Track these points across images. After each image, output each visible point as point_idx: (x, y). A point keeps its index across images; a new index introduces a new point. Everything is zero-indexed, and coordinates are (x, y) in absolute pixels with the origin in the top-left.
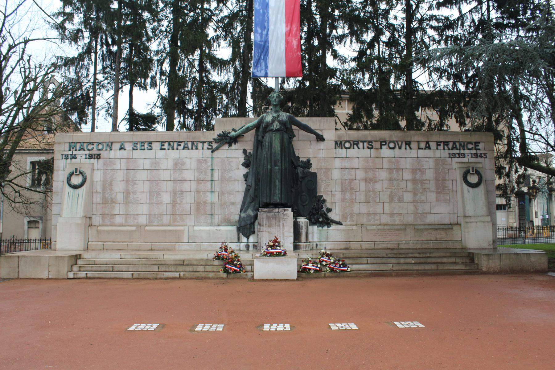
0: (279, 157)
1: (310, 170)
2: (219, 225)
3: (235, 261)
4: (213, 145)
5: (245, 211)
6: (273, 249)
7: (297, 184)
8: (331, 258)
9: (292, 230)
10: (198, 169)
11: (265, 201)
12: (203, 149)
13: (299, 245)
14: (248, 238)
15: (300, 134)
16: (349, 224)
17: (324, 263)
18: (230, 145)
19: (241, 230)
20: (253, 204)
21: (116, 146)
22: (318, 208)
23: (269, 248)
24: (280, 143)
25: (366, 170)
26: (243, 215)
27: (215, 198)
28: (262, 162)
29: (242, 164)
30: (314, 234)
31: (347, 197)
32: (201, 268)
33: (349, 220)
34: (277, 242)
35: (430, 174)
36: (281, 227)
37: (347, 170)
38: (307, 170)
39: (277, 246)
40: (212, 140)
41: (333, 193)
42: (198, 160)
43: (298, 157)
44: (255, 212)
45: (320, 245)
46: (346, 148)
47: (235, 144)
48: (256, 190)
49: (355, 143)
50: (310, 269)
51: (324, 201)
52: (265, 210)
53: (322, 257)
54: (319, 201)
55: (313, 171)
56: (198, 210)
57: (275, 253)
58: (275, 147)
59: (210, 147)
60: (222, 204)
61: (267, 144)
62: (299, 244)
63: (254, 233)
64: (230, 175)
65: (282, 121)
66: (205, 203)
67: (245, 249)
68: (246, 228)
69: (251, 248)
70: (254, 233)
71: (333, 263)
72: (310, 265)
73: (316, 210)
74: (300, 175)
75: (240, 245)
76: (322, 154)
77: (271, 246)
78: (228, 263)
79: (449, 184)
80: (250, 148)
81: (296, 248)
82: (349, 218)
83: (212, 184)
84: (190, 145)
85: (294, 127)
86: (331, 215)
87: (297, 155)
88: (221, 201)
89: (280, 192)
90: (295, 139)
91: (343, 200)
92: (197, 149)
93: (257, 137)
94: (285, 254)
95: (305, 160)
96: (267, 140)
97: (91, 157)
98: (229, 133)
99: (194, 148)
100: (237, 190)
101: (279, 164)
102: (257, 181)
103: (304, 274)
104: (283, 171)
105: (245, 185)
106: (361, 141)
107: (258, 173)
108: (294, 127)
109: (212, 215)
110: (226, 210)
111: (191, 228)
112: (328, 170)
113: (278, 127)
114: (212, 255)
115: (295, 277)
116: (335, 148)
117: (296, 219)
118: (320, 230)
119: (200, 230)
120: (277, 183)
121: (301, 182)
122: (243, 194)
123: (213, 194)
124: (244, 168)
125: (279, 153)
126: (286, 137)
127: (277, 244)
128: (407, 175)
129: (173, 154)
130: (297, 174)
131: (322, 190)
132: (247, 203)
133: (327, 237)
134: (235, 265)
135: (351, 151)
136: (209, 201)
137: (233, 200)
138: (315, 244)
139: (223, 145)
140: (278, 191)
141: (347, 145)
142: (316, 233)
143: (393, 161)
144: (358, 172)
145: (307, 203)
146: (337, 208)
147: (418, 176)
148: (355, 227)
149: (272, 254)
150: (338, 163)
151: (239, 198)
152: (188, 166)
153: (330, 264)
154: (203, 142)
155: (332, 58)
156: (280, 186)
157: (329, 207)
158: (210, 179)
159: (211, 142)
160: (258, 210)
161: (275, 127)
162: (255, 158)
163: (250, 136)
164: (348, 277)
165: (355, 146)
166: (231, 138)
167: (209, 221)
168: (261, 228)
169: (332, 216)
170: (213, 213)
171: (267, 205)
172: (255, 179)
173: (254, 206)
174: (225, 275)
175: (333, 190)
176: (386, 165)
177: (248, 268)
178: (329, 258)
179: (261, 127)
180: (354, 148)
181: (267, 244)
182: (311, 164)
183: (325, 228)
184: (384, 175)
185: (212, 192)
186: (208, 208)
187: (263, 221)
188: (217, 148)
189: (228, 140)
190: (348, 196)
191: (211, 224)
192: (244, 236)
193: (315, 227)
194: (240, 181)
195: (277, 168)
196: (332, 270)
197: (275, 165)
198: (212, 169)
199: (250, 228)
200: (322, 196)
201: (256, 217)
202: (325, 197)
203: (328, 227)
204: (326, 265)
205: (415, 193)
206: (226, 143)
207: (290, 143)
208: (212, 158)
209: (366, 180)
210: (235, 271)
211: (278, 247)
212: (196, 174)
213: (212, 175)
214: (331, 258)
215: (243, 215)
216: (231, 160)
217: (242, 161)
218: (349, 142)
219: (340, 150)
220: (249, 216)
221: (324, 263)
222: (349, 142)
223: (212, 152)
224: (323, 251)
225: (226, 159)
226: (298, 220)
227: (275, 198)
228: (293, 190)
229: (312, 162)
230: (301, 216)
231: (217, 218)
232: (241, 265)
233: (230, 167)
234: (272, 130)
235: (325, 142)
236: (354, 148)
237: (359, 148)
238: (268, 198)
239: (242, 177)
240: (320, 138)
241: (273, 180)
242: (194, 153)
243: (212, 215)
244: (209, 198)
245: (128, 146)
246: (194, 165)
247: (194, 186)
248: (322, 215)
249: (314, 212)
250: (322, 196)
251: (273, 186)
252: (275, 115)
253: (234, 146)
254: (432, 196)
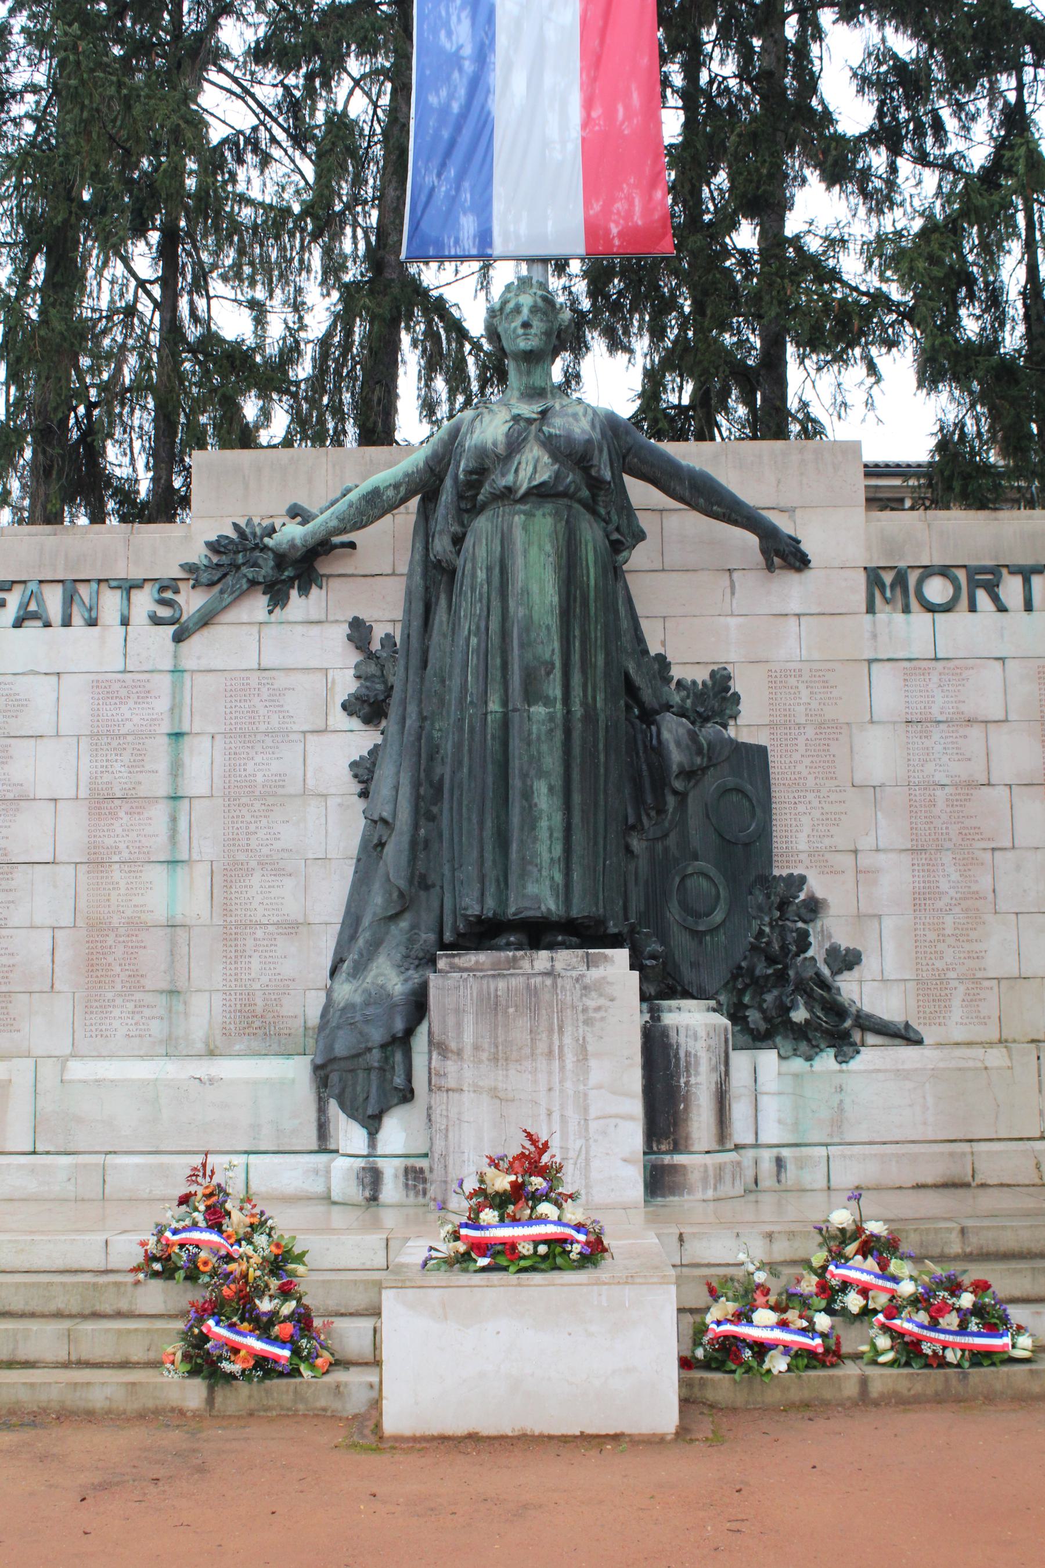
0: (550, 648)
1: (731, 732)
2: (211, 1053)
3: (261, 1292)
4: (180, 599)
5: (359, 969)
6: (515, 1221)
7: (661, 811)
8: (895, 1266)
9: (634, 1079)
10: (102, 737)
11: (475, 910)
12: (125, 622)
13: (674, 1169)
14: (372, 1123)
16: (958, 1035)
17: (854, 1302)
18: (278, 597)
19: (334, 1078)
20: (404, 924)
22: (784, 948)
23: (489, 1216)
24: (558, 568)
26: (345, 991)
27: (191, 898)
28: (455, 683)
29: (344, 707)
30: (764, 1101)
31: (944, 886)
32: (43, 1339)
33: (957, 1012)
34: (542, 1171)
36: (570, 1058)
37: (936, 733)
38: (710, 730)
39: (537, 1198)
40: (180, 574)
41: (864, 861)
42: (96, 685)
43: (662, 661)
44: (415, 977)
45: (801, 1163)
46: (931, 608)
47: (304, 591)
48: (417, 846)
50: (761, 1349)
51: (814, 907)
52: (471, 958)
53: (838, 1257)
54: (783, 905)
55: (746, 737)
56: (94, 968)
57: (525, 1249)
58: (526, 592)
59: (164, 612)
60: (233, 933)
61: (481, 575)
62: (679, 1159)
63: (407, 1095)
64: (275, 767)
65: (569, 439)
66: (137, 926)
67: (356, 1193)
68: (366, 1069)
69: (391, 1190)
70: (407, 1095)
71: (916, 1302)
72: (764, 1316)
73: (771, 960)
74: (676, 757)
75: (328, 1172)
76: (793, 645)
77: (501, 1201)
78: (215, 1309)
80: (387, 611)
82: (956, 1003)
83: (174, 819)
84: (53, 600)
85: (640, 493)
86: (855, 990)
87: (654, 648)
88: (227, 911)
89: (558, 850)
90: (639, 557)
91: (922, 899)
92: (92, 623)
93: (427, 549)
94: (595, 1251)
95: (700, 675)
96: (481, 552)
98: (271, 531)
99: (77, 619)
101: (555, 690)
102: (429, 795)
103: (720, 1385)
104: (578, 726)
105: (363, 822)
106: (1014, 570)
107: (433, 753)
108: (640, 493)
109: (173, 992)
110: (255, 964)
111: (48, 1071)
113: (543, 476)
114: (128, 1249)
115: (664, 1415)
116: (871, 609)
117: (655, 1014)
118: (796, 1076)
119: (98, 1082)
120: (545, 800)
121: (682, 797)
122: (349, 871)
123: (181, 871)
124: (355, 723)
125: (553, 621)
126: (591, 535)
127: (538, 1182)
130: (658, 751)
131: (802, 846)
132: (366, 922)
133: (838, 1119)
134: (263, 1326)
135: (959, 620)
136: (160, 915)
137: (292, 909)
138: (767, 1157)
139: (242, 595)
140: (547, 848)
141: (937, 590)
142: (772, 1087)
144: (1000, 738)
145: (718, 916)
146: (889, 946)
148: (996, 1057)
149: (504, 1257)
150: (887, 691)
151: (326, 898)
152: (40, 720)
153: (892, 1311)
154: (129, 587)
155: (823, 186)
156: (558, 818)
157: (844, 941)
158: (163, 789)
159: (168, 586)
160: (432, 961)
161: (525, 474)
162: (415, 661)
163: (389, 544)
164: (1023, 1399)
165: (982, 597)
166: (281, 559)
167: (156, 1028)
168: (451, 1066)
170: (182, 984)
171: (484, 933)
172: (416, 785)
173: (411, 941)
174: (193, 1393)
175: (866, 843)
177: (352, 1336)
178: (883, 1266)
179: (448, 482)
180: (973, 608)
181: (471, 1184)
182: (736, 698)
183: (826, 1061)
185: (173, 863)
186: (153, 954)
187: (459, 1025)
188: (206, 619)
189: (267, 568)
190: (949, 877)
191: (171, 1047)
192: (352, 1113)
193: (768, 1058)
194: (332, 802)
195: (539, 710)
196: (910, 1350)
197: (532, 694)
198: (177, 736)
199: (385, 1069)
200: (803, 879)
201: (418, 1006)
202: (817, 885)
203: (842, 1058)
204: (867, 1312)
206: (253, 583)
207: (614, 572)
208: (176, 671)
210: (264, 1366)
211: (545, 1208)
212: (85, 759)
213: (176, 768)
214: (895, 1266)
215: (345, 991)
216: (282, 680)
217: (347, 685)
218: (944, 571)
219: (899, 617)
220: (377, 998)
221: (854, 1302)
222: (944, 571)
223: (179, 638)
224: (842, 1217)
225: (254, 679)
226: (669, 1019)
227: (532, 889)
228: (637, 844)
229: (737, 686)
230: (687, 995)
231: (203, 1014)
232: (303, 1320)
233: (275, 722)
234: (507, 494)
235: (808, 575)
236: (973, 608)
237: (1002, 609)
238: (491, 889)
239: (346, 774)
240: (784, 554)
241: (516, 783)
242: (82, 649)
243: (173, 992)
244: (158, 895)
246: (77, 711)
247: (72, 831)
248: (802, 988)
249: (762, 969)
250: (803, 879)
251: (515, 820)
252: (529, 410)
253: (298, 605)
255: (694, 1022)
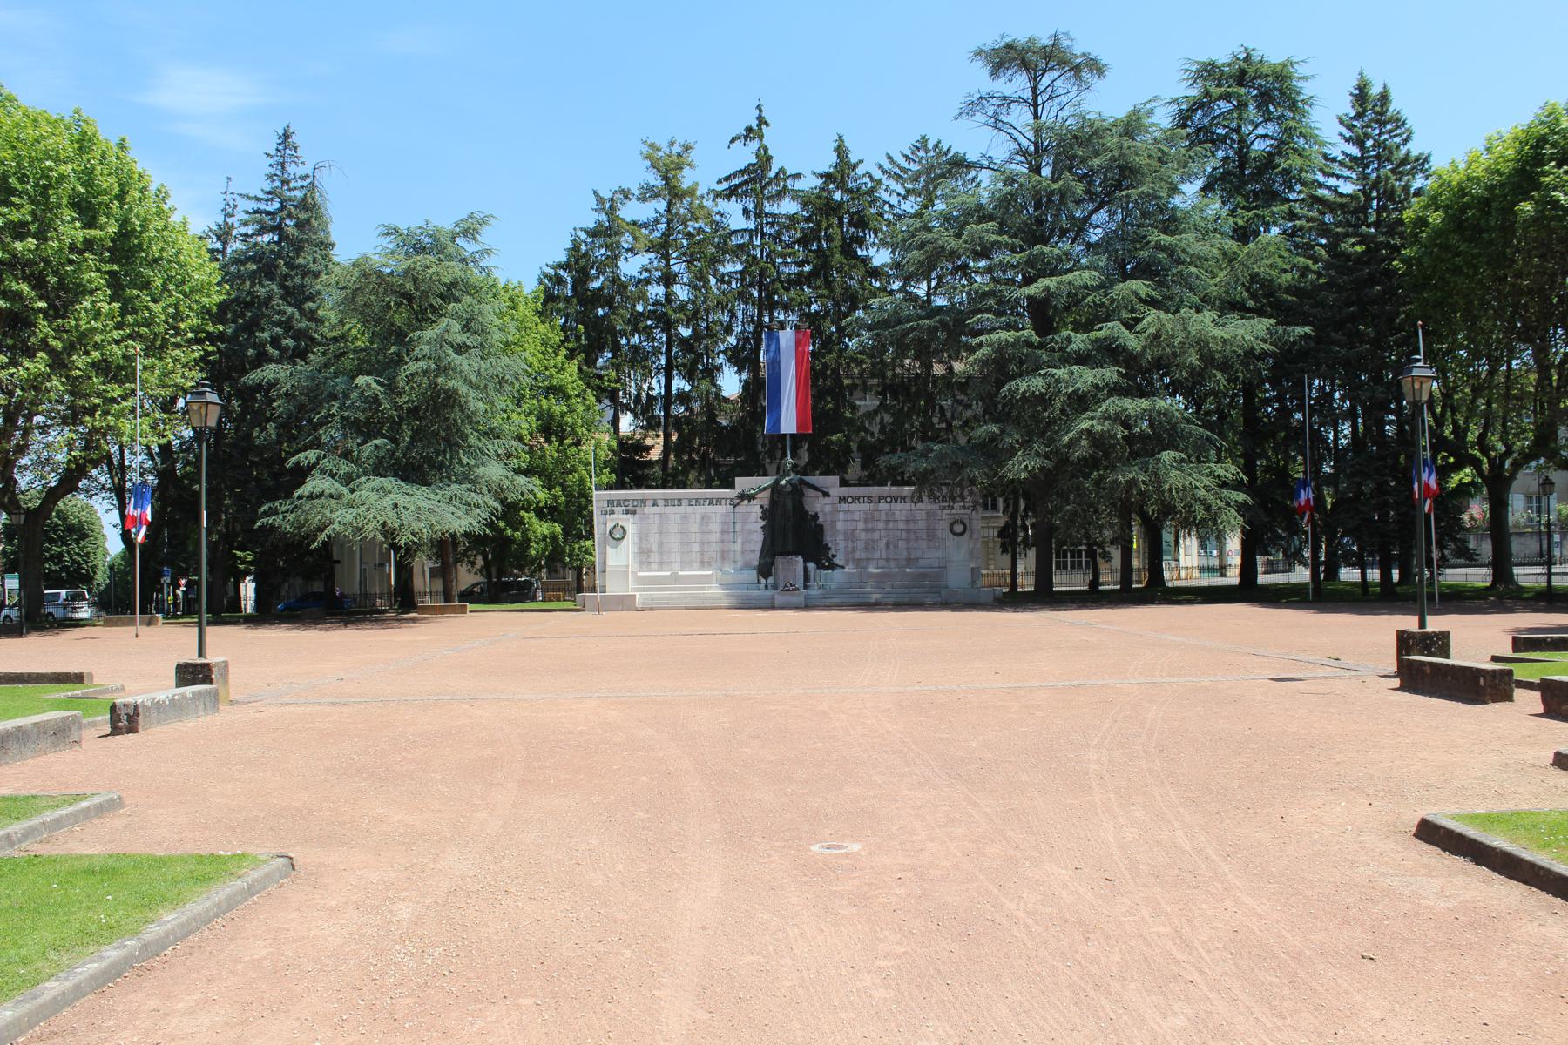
10: (724, 523)
15: (810, 493)
21: (650, 503)
25: (866, 521)
35: (922, 525)
49: (856, 499)
56: (723, 558)
79: (939, 533)
80: (766, 503)
81: (806, 587)
97: (627, 512)
100: (757, 540)
112: (834, 522)
128: (902, 526)
129: (700, 509)
143: (890, 513)
147: (912, 526)
151: (758, 547)
163: (767, 494)
169: (838, 561)
176: (883, 517)
184: (881, 525)
205: (908, 540)
209: (867, 530)
240: (826, 494)
245: (660, 503)
254: (923, 544)
255: (811, 565)
